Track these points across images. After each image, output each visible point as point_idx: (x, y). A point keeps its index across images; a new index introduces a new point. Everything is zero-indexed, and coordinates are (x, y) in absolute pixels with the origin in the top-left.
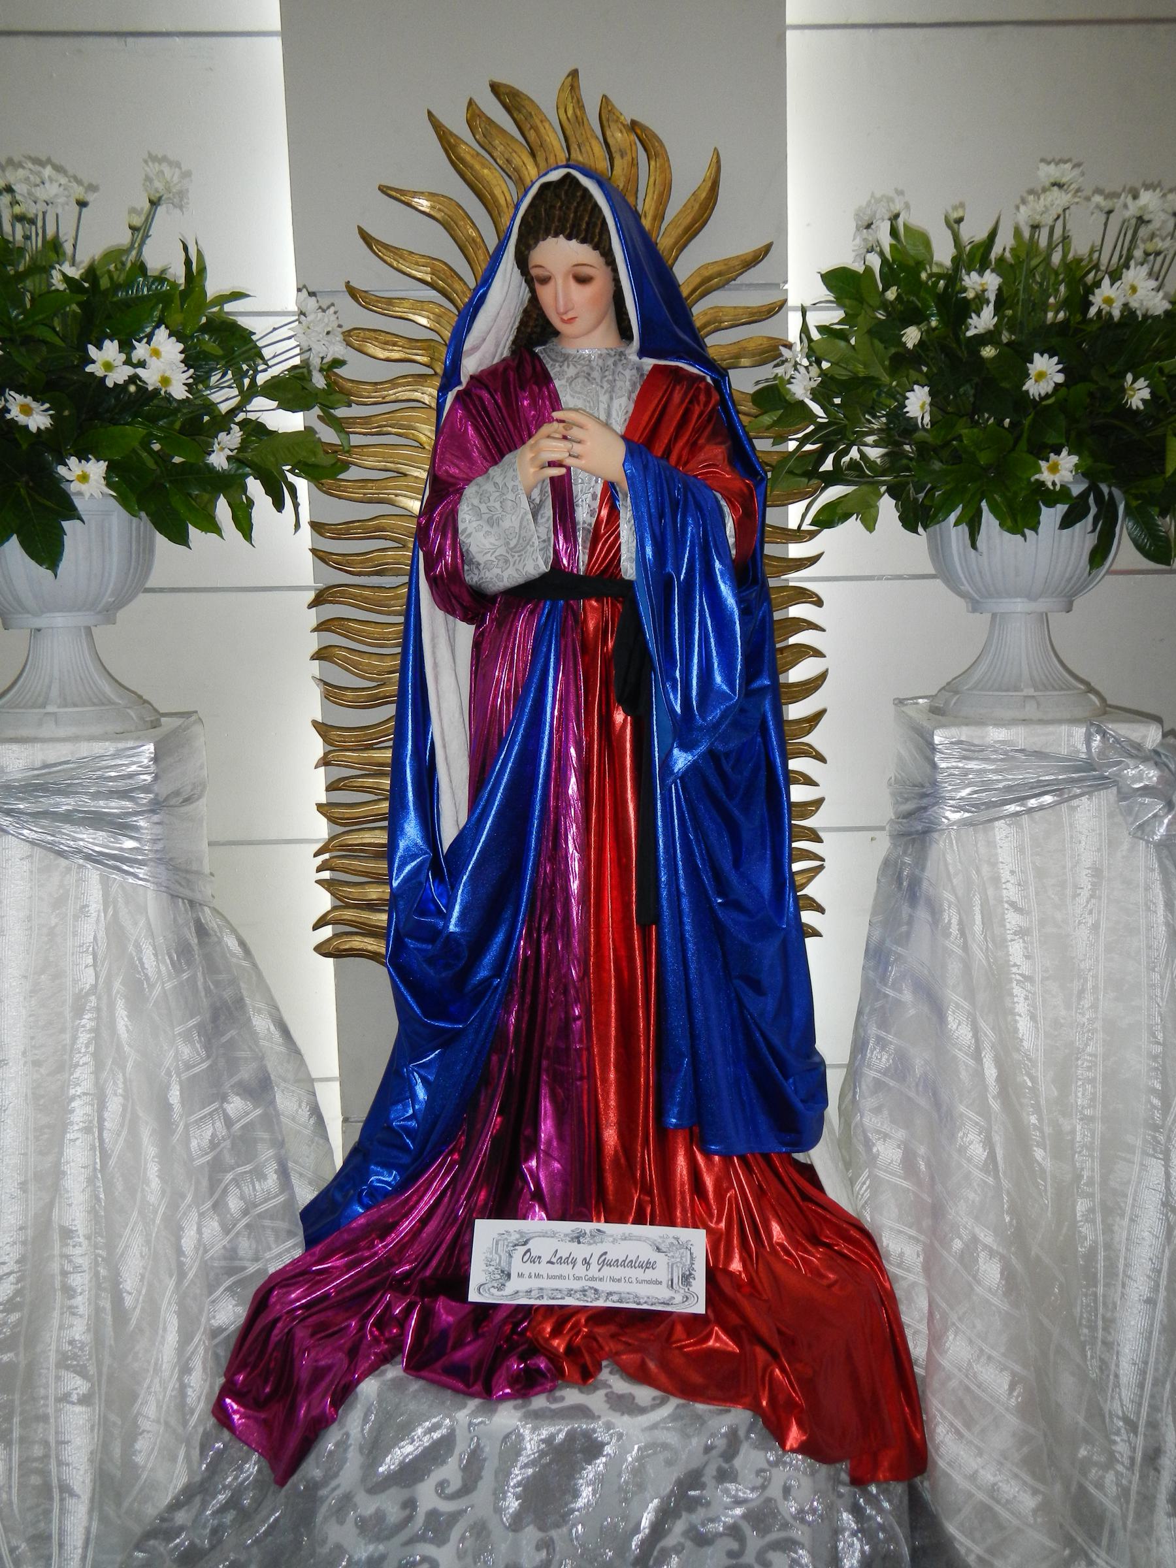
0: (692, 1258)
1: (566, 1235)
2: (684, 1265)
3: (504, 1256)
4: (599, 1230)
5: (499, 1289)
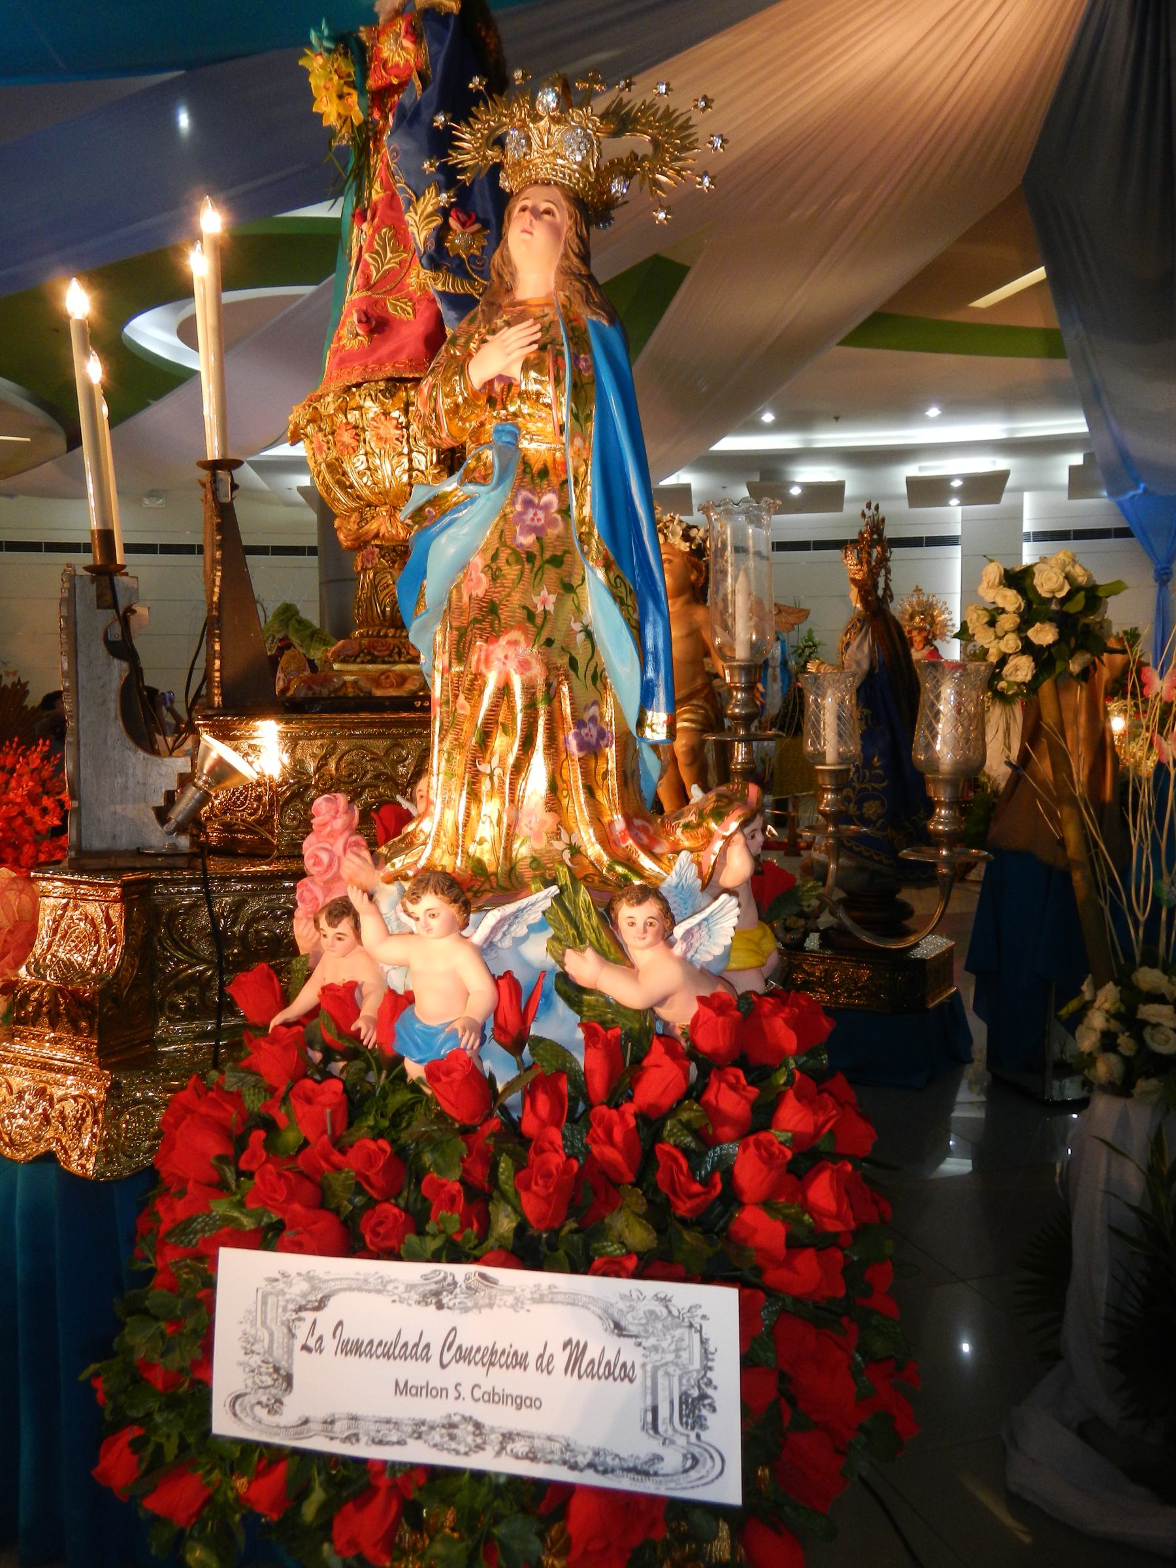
0: (706, 1354)
2: (685, 1373)
4: (483, 1276)
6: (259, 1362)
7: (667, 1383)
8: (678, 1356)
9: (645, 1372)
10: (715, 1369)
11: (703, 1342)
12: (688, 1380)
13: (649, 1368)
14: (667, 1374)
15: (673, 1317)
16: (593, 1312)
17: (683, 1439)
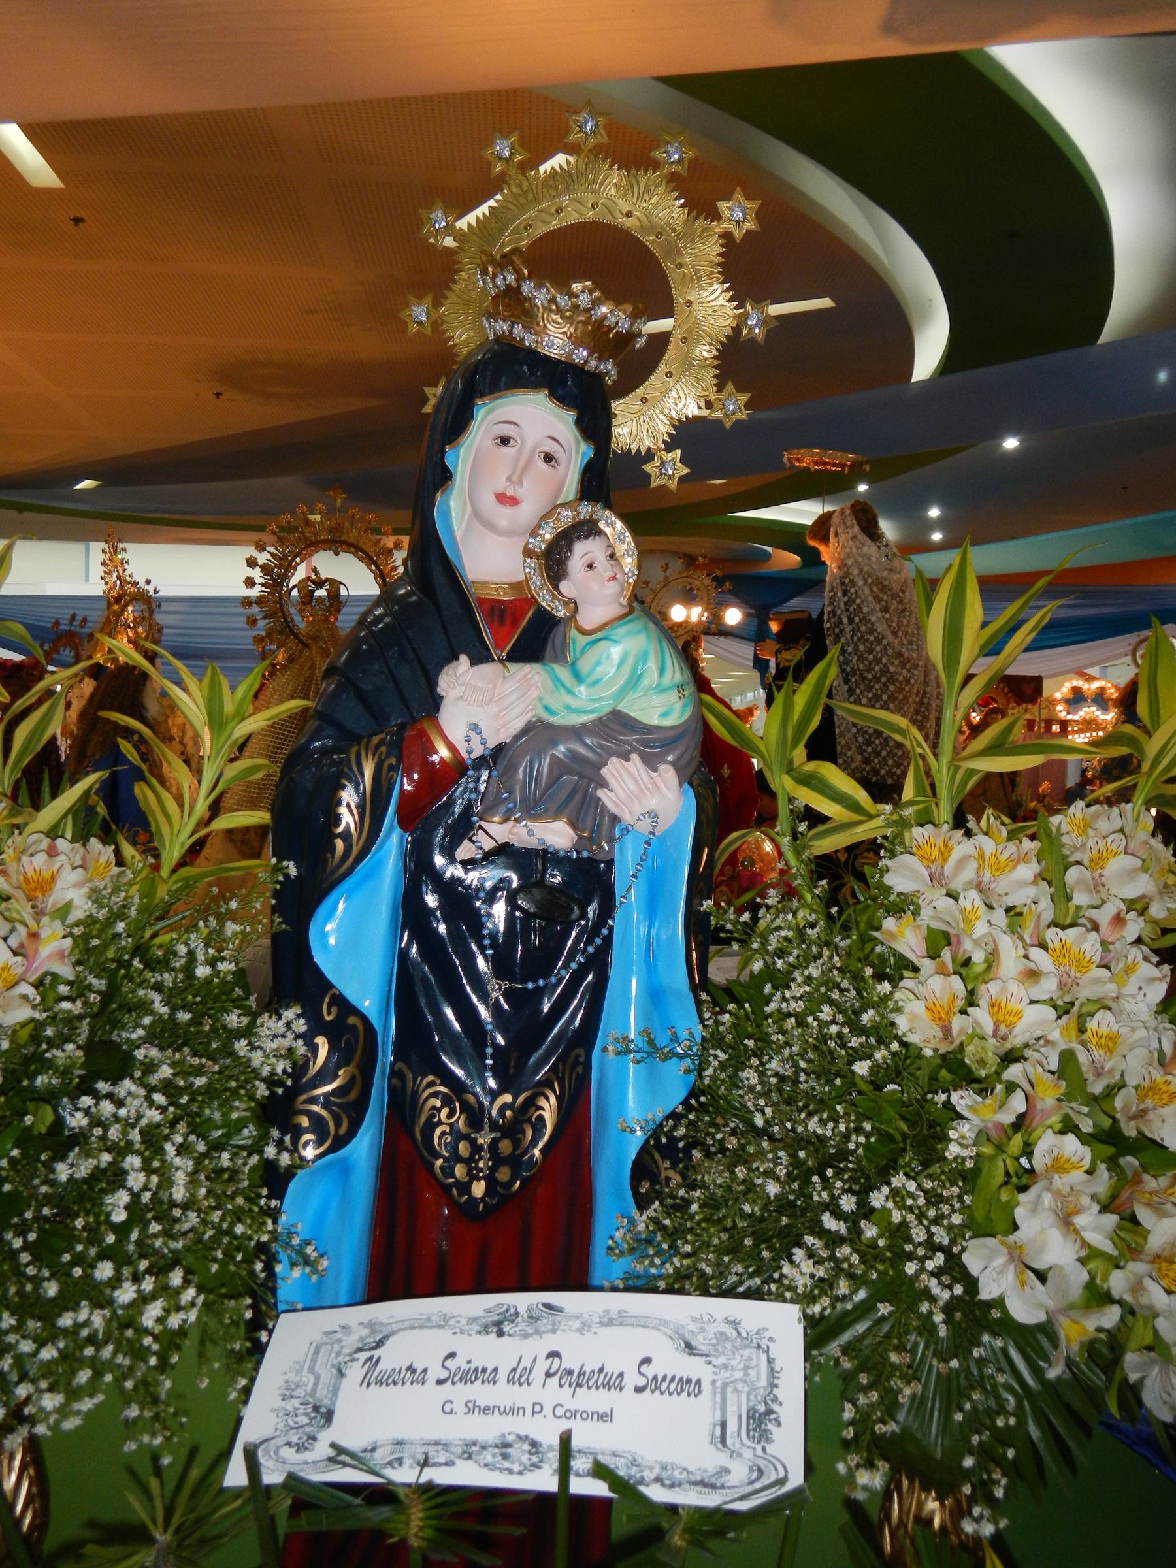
0: (772, 1373)
1: (472, 1320)
2: (753, 1389)
3: (326, 1374)
5: (300, 1448)
6: (297, 1405)
7: (735, 1399)
8: (746, 1374)
9: (715, 1388)
10: (781, 1386)
11: (770, 1361)
12: (756, 1397)
13: (718, 1384)
14: (736, 1390)
15: (743, 1338)
16: (664, 1333)
17: (750, 1451)
